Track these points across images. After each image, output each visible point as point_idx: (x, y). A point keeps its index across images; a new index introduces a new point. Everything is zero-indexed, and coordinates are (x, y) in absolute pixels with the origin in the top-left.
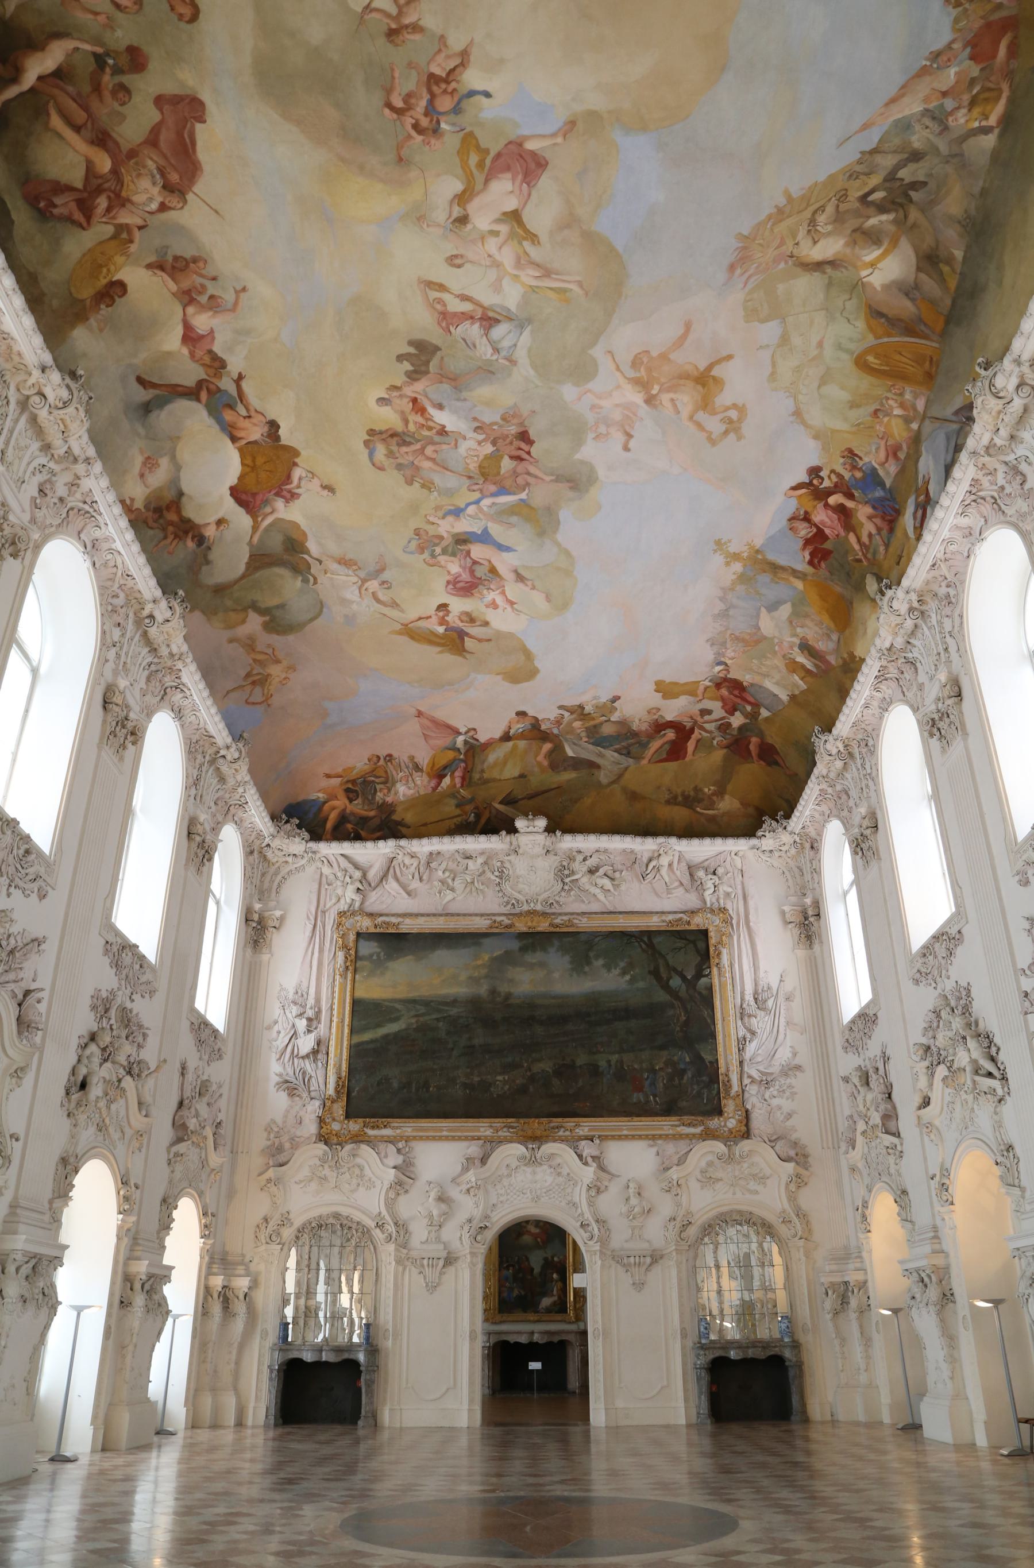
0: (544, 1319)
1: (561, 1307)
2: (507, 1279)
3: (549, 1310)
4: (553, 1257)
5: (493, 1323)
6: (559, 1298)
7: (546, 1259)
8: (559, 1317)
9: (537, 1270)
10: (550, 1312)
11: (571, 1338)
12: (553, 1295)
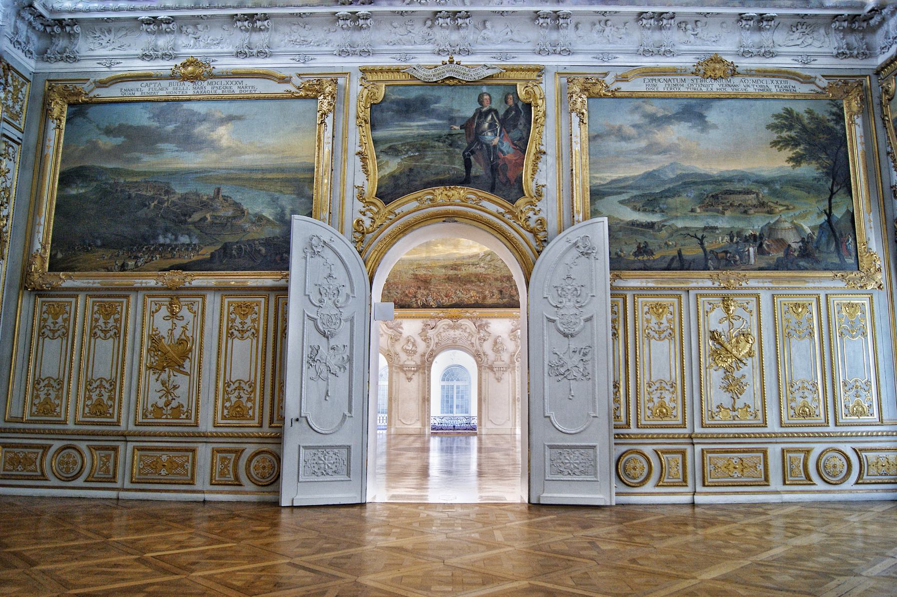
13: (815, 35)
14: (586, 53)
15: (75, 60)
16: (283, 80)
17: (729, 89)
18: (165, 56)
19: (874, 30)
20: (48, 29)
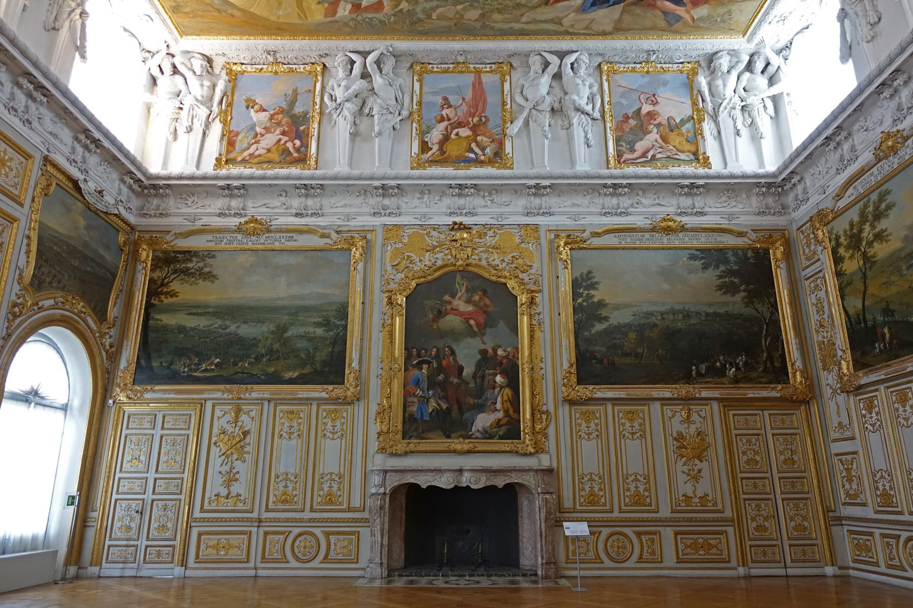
0: (480, 447)
1: (510, 429)
2: (418, 383)
3: (487, 435)
4: (495, 351)
5: (392, 455)
6: (506, 412)
7: (483, 352)
8: (507, 445)
9: (468, 371)
10: (491, 437)
11: (529, 480)
13: (738, 199)
14: (563, 214)
15: (167, 215)
16: (323, 236)
17: (677, 242)
18: (236, 215)
19: (785, 193)
20: (146, 191)
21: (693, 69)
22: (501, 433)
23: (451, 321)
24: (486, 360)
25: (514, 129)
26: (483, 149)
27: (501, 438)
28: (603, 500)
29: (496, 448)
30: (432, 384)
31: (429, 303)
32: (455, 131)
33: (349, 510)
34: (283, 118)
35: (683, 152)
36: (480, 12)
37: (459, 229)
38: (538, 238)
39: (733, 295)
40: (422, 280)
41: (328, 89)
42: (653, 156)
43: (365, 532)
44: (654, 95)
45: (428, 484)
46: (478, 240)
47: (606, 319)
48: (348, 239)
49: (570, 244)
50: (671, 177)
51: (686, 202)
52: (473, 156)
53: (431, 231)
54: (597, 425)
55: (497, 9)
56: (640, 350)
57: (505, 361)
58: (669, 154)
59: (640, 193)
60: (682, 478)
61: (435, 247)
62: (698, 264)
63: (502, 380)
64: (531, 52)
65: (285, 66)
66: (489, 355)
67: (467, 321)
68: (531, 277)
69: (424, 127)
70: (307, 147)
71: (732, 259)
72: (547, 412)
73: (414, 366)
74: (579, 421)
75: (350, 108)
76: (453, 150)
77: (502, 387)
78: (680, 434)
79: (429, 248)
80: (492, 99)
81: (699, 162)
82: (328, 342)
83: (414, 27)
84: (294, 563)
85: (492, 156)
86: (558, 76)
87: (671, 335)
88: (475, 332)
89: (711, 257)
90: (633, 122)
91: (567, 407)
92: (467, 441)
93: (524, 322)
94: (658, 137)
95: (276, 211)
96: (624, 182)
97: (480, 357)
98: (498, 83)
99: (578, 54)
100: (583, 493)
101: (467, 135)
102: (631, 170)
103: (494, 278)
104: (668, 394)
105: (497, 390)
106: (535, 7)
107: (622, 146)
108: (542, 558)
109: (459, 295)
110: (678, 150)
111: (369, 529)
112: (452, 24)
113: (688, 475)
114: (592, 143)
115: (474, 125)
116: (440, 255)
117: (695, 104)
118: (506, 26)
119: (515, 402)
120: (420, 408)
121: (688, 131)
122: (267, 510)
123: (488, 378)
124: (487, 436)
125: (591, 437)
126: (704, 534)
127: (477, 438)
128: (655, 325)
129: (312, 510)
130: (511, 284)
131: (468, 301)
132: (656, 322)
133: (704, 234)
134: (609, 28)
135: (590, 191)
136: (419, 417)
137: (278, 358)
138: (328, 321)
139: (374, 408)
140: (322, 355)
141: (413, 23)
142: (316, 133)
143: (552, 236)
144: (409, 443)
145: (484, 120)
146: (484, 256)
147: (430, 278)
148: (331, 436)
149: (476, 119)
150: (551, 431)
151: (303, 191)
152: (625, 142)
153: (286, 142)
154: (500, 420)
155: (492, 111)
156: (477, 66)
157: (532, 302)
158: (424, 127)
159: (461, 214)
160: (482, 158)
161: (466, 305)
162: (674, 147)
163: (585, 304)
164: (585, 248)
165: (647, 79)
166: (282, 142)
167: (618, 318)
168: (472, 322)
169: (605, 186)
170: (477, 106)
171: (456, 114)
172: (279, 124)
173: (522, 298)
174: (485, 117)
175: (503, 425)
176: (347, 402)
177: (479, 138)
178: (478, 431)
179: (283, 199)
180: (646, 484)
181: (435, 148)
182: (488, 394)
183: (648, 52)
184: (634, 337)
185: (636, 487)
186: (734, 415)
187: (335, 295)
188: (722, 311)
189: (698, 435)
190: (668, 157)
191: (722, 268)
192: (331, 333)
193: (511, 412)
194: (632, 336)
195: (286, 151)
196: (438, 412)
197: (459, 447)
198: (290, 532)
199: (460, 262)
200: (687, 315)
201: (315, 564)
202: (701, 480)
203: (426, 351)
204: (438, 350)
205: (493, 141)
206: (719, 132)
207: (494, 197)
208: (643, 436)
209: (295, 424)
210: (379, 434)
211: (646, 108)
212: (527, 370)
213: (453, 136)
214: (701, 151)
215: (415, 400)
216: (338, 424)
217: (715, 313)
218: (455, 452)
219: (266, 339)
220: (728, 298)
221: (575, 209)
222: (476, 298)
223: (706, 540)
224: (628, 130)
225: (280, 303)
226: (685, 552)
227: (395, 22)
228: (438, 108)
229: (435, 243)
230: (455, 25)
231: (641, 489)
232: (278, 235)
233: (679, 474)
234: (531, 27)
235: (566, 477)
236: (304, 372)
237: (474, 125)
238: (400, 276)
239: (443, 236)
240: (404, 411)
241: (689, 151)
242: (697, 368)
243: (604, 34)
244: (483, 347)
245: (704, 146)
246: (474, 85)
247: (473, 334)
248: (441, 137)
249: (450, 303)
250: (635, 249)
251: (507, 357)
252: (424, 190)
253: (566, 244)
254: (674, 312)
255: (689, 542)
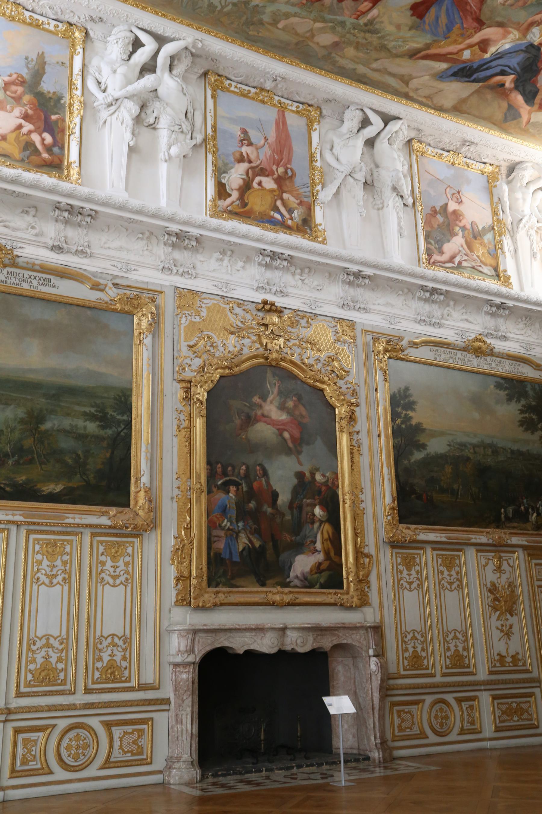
1: (330, 576)
2: (224, 511)
3: (308, 583)
4: (313, 475)
5: (198, 608)
6: (327, 554)
7: (300, 475)
8: (330, 595)
9: (284, 498)
10: (311, 586)
12: (315, 551)
21: (492, 173)
22: (322, 581)
23: (262, 431)
24: (304, 485)
25: (325, 195)
26: (290, 211)
27: (322, 587)
28: (425, 662)
29: (318, 599)
30: (242, 513)
31: (236, 404)
32: (258, 179)
33: (142, 687)
34: (24, 93)
35: (486, 265)
36: (336, 39)
37: (270, 311)
38: (354, 338)
39: (533, 433)
40: (227, 371)
41: (92, 70)
42: (460, 263)
43: (162, 720)
44: (459, 192)
45: (246, 648)
46: (289, 329)
47: (424, 446)
48: (136, 299)
49: (389, 351)
50: (487, 292)
51: (490, 322)
52: (278, 216)
53: (235, 307)
54: (417, 572)
55: (358, 43)
56: (455, 487)
57: (323, 488)
58: (474, 264)
59: (452, 303)
60: (496, 634)
61: (240, 329)
62: (503, 394)
63: (322, 513)
64: (352, 103)
65: (27, 14)
66: (306, 480)
67: (280, 432)
68: (349, 386)
69: (220, 163)
70: (62, 148)
71: (531, 393)
72: (368, 556)
73: (219, 488)
74: (400, 567)
75: (129, 109)
76: (257, 203)
77: (321, 522)
78: (493, 584)
79: (232, 329)
80: (298, 149)
81: (499, 280)
82: (105, 444)
83: (246, 27)
84: (60, 774)
85: (300, 223)
86: (370, 143)
87: (482, 471)
88: (290, 449)
89: (513, 387)
90: (440, 219)
91: (388, 550)
92: (286, 590)
93: (343, 442)
94: (463, 241)
95: (18, 234)
96: (444, 288)
97: (295, 481)
98: (304, 129)
99: (400, 122)
100: (406, 655)
101: (269, 189)
102: (441, 274)
103: (311, 382)
104: (483, 539)
105: (316, 525)
106: (397, 56)
107: (431, 243)
108: (375, 738)
109: (271, 397)
110: (481, 261)
111: (166, 713)
112: (295, 41)
113: (502, 631)
114: (406, 233)
115: (279, 177)
116: (247, 341)
117: (495, 213)
118: (350, 65)
119: (335, 540)
120: (228, 545)
121: (490, 243)
122: (19, 694)
123: (306, 509)
124: (307, 583)
125: (413, 586)
126: (517, 697)
127: (296, 587)
128: (468, 459)
129: (88, 691)
130: (328, 391)
131: (282, 407)
132: (470, 455)
133: (508, 362)
134: (448, 103)
135: (406, 291)
136: (227, 557)
137: (31, 461)
138: (106, 414)
139: (170, 542)
140: (98, 460)
141: (249, 23)
142: (77, 130)
143: (369, 338)
144: (217, 593)
145: (290, 173)
146: (298, 351)
147: (236, 369)
148: (111, 581)
149: (281, 170)
150: (373, 578)
151: (66, 214)
152: (434, 240)
153: (30, 132)
154: (320, 564)
155: (298, 163)
156: (283, 100)
157: (352, 418)
158: (220, 163)
159: (270, 291)
160: (290, 222)
161: (279, 412)
162: (478, 257)
163: (403, 426)
164: (402, 359)
165: (452, 171)
166: (25, 130)
167: (436, 446)
168: (286, 435)
169: (423, 288)
170: (281, 153)
171: (258, 157)
172: (18, 100)
173: (341, 411)
174: (292, 170)
175: (324, 571)
176: (137, 532)
177: (285, 196)
178: (297, 577)
179: (29, 219)
180: (464, 642)
181: (235, 195)
182: (307, 529)
183: (466, 143)
184: (450, 470)
185: (456, 646)
186: (536, 565)
187: (112, 376)
188: (524, 449)
189: (509, 586)
190: (473, 268)
191: (523, 402)
192: (109, 432)
193: (332, 554)
194: (448, 469)
195: (29, 146)
196: (249, 551)
197: (277, 598)
198: (54, 726)
199: (274, 355)
200: (495, 450)
201: (92, 771)
202: (513, 637)
203: (234, 468)
204: (247, 468)
205: (301, 203)
206: (516, 250)
207: (305, 276)
208: (420, 586)
209: (58, 563)
210: (178, 580)
211: (452, 206)
212: (348, 502)
213: (255, 185)
214: (501, 268)
215: (222, 533)
216: (121, 563)
217: (518, 451)
218: (272, 604)
219: (13, 430)
220: (528, 436)
221: (389, 310)
222: (290, 404)
223: (518, 704)
224: (436, 226)
225: (32, 377)
226: (501, 719)
227: (228, 14)
228: (236, 143)
229: (240, 324)
230: (297, 44)
231: (460, 648)
232: (27, 273)
233: (494, 629)
234: (376, 76)
235: (390, 636)
236: (70, 485)
237: (279, 177)
238: (198, 362)
239: (249, 316)
240: (209, 548)
241: (491, 266)
242: (505, 511)
243: (440, 109)
244: (299, 468)
245: (505, 263)
246: (277, 124)
247: (288, 452)
248: (241, 182)
249: (261, 407)
250: (449, 368)
251: (326, 484)
252: (228, 250)
253: (386, 351)
254: (483, 445)
255: (504, 707)
